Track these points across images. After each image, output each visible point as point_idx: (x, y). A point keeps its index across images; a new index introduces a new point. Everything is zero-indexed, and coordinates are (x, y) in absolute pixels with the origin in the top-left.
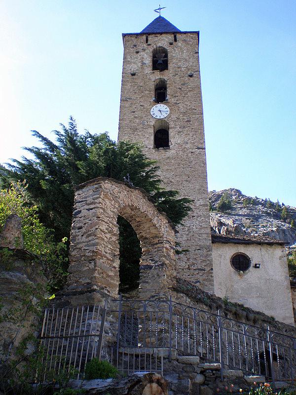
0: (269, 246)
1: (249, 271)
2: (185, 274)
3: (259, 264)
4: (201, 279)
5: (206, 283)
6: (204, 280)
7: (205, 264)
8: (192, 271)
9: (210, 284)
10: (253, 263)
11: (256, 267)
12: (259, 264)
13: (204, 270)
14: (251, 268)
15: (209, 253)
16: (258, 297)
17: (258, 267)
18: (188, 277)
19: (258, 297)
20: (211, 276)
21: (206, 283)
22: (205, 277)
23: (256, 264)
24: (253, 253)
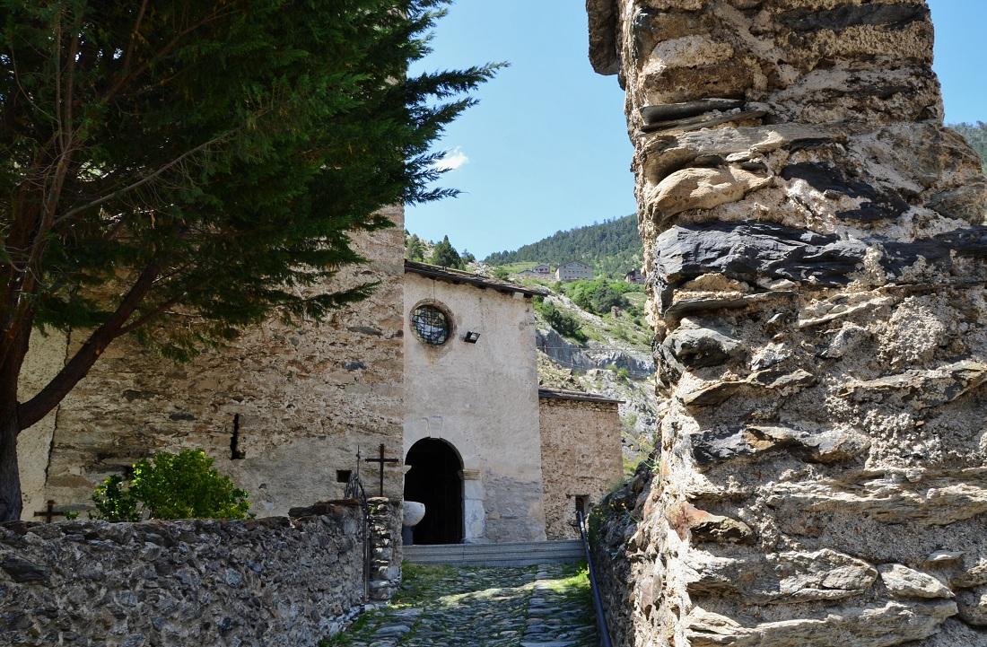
0: (500, 294)
1: (451, 349)
2: (322, 338)
3: (478, 335)
4: (367, 358)
5: (382, 371)
6: (375, 363)
7: (383, 317)
8: (343, 333)
9: (394, 376)
10: (461, 330)
11: (468, 339)
12: (478, 335)
13: (379, 334)
14: (456, 342)
15: (396, 287)
16: (466, 413)
17: (474, 342)
18: (333, 348)
19: (466, 413)
20: (398, 354)
21: (382, 371)
22: (379, 353)
23: (470, 334)
24: (459, 303)
